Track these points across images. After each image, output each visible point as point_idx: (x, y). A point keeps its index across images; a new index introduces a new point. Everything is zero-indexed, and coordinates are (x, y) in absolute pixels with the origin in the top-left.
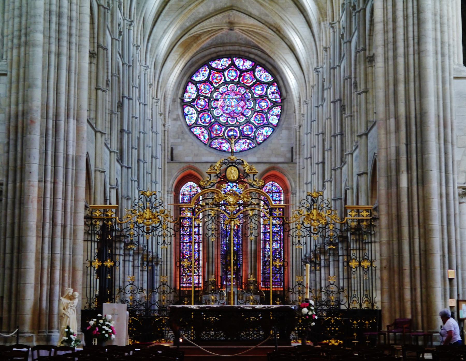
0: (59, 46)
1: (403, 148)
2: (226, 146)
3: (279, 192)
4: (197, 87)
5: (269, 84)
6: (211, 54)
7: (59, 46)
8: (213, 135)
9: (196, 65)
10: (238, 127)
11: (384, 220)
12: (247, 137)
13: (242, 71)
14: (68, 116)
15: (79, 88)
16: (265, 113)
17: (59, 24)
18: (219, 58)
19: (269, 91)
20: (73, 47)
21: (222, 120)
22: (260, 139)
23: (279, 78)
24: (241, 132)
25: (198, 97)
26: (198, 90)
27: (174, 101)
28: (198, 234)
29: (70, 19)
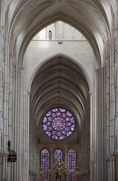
0: (23, 137)
1: (95, 158)
2: (57, 138)
3: (74, 153)
4: (47, 118)
5: (71, 117)
6: (52, 107)
7: (23, 137)
8: (52, 134)
9: (47, 111)
10: (61, 131)
11: (91, 173)
12: (64, 135)
13: (62, 113)
14: (25, 152)
15: (27, 145)
16: (70, 127)
17: (23, 132)
18: (55, 108)
19: (71, 120)
20: (26, 137)
21: (55, 129)
22: (68, 135)
23: (74, 115)
24: (62, 133)
25: (47, 121)
26: (47, 119)
27: (40, 123)
28: (47, 167)
29: (25, 131)
